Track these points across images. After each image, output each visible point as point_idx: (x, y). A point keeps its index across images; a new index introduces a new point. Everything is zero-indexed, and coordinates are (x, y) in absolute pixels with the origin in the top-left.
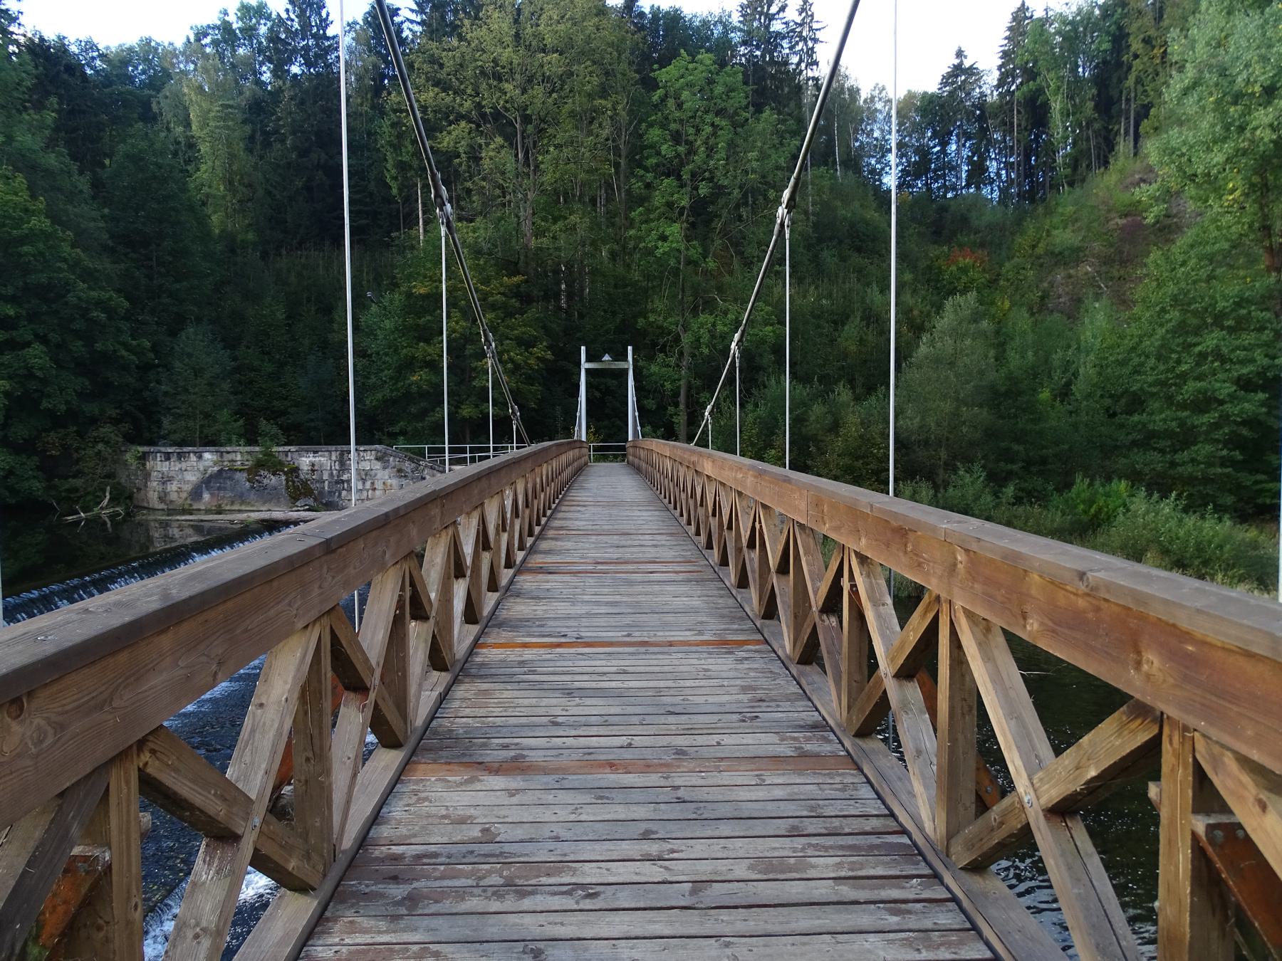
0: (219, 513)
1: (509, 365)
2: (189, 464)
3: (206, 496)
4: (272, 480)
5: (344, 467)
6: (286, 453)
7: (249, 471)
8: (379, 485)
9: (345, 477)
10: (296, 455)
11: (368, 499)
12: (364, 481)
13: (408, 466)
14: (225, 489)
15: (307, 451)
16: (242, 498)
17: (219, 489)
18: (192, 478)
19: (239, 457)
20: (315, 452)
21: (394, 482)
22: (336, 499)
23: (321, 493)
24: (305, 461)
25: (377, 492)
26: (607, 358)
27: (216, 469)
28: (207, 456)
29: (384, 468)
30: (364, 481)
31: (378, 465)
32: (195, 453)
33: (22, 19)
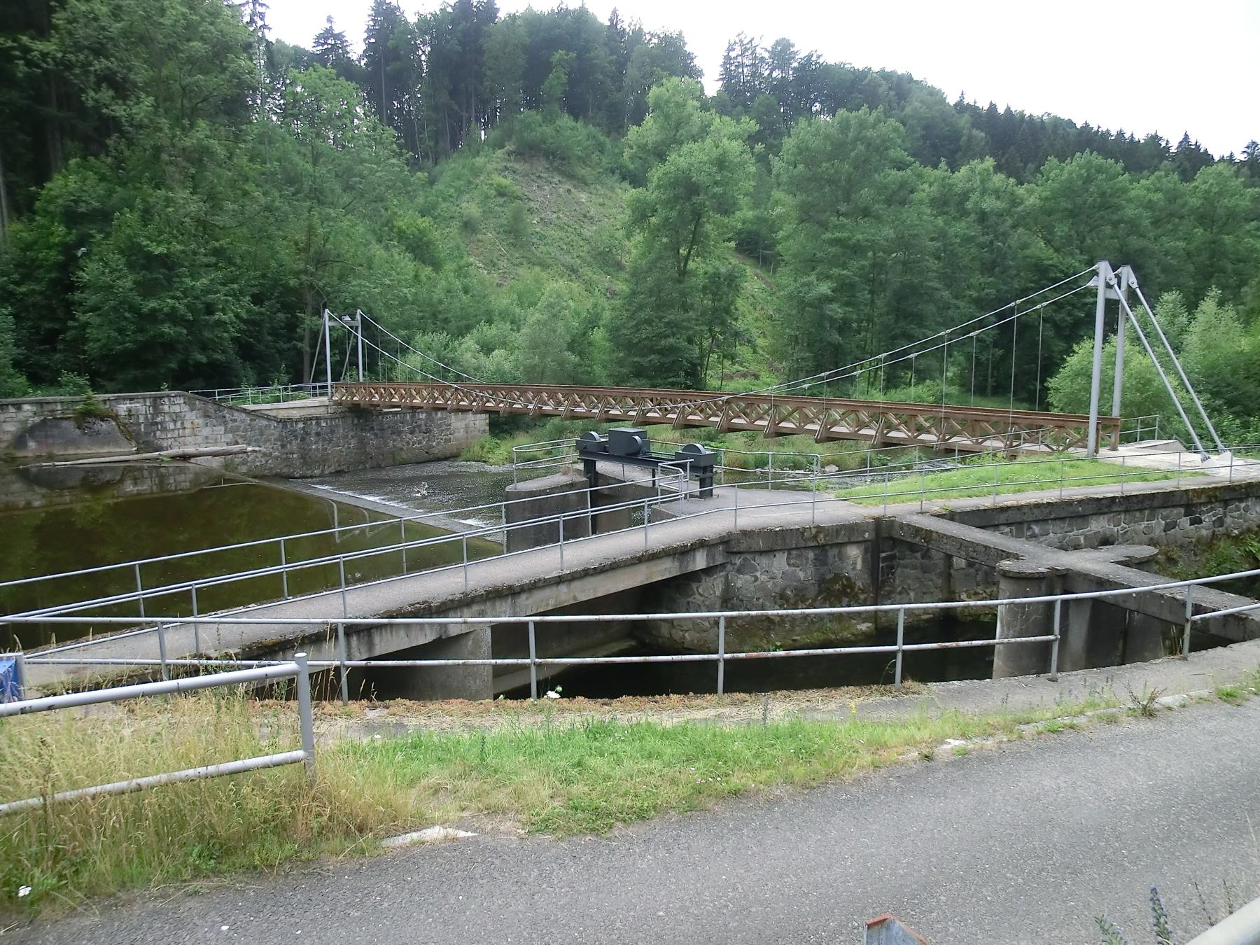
0: (51, 457)
2: (7, 415)
3: (32, 444)
4: (104, 426)
5: (157, 411)
6: (105, 401)
7: (76, 419)
8: (188, 425)
9: (159, 420)
10: (113, 403)
12: (175, 422)
13: (211, 408)
14: (53, 437)
15: (124, 399)
16: (73, 442)
17: (46, 437)
18: (11, 428)
19: (59, 407)
20: (131, 399)
21: (200, 421)
22: (151, 438)
23: (138, 434)
24: (122, 408)
25: (187, 431)
27: (37, 420)
28: (26, 407)
29: (192, 410)
30: (175, 422)
31: (186, 408)
32: (13, 405)
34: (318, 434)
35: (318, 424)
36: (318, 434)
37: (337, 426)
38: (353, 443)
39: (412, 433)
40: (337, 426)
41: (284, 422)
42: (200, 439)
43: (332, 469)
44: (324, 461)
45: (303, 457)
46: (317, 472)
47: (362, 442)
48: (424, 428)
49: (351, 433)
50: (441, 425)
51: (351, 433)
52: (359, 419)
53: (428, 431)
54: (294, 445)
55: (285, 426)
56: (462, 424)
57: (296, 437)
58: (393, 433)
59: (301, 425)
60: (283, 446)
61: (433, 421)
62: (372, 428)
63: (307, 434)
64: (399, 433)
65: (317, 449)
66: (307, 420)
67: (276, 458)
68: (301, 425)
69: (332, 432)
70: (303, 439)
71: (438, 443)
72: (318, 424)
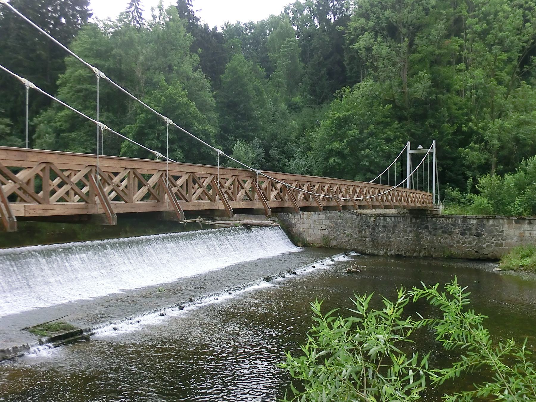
1: (380, 153)
11: (300, 219)
26: (420, 147)
33: (201, 20)
34: (384, 227)
35: (385, 220)
36: (384, 227)
37: (399, 222)
38: (411, 236)
39: (463, 234)
40: (399, 222)
41: (361, 216)
42: (311, 222)
43: (393, 253)
44: (387, 245)
45: (373, 241)
46: (382, 253)
47: (417, 236)
48: (474, 232)
49: (410, 229)
50: (492, 231)
51: (410, 229)
52: (416, 218)
53: (479, 235)
54: (368, 232)
55: (362, 219)
56: (517, 232)
57: (369, 227)
58: (443, 232)
59: (372, 219)
60: (360, 232)
61: (484, 227)
62: (427, 227)
63: (378, 226)
64: (450, 233)
65: (383, 237)
66: (377, 216)
67: (355, 239)
68: (372, 219)
69: (395, 226)
70: (373, 229)
71: (487, 246)
72: (385, 220)
